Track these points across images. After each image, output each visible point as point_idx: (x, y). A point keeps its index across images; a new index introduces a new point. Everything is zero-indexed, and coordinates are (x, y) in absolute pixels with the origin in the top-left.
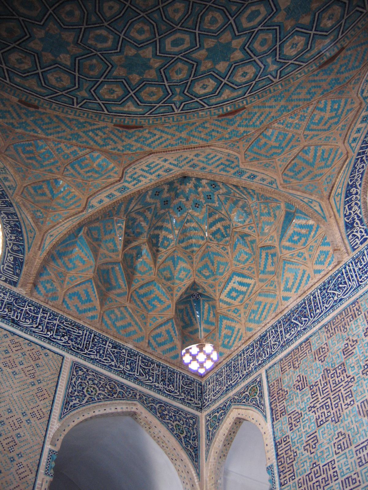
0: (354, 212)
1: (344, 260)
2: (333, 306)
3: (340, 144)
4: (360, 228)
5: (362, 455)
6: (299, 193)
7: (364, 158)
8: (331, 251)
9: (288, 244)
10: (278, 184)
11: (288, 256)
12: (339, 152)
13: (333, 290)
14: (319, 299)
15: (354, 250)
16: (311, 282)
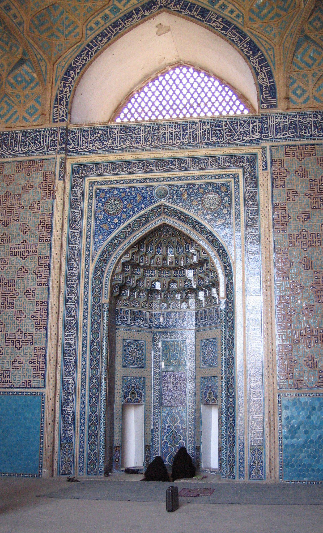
0: (66, 92)
1: (46, 125)
2: (26, 153)
3: (80, 23)
4: (64, 109)
5: (13, 250)
6: (36, 46)
7: (90, 53)
8: (39, 111)
9: (12, 81)
10: (25, 28)
11: (9, 92)
12: (77, 30)
13: (30, 141)
14: (19, 140)
15: (54, 122)
16: (18, 124)
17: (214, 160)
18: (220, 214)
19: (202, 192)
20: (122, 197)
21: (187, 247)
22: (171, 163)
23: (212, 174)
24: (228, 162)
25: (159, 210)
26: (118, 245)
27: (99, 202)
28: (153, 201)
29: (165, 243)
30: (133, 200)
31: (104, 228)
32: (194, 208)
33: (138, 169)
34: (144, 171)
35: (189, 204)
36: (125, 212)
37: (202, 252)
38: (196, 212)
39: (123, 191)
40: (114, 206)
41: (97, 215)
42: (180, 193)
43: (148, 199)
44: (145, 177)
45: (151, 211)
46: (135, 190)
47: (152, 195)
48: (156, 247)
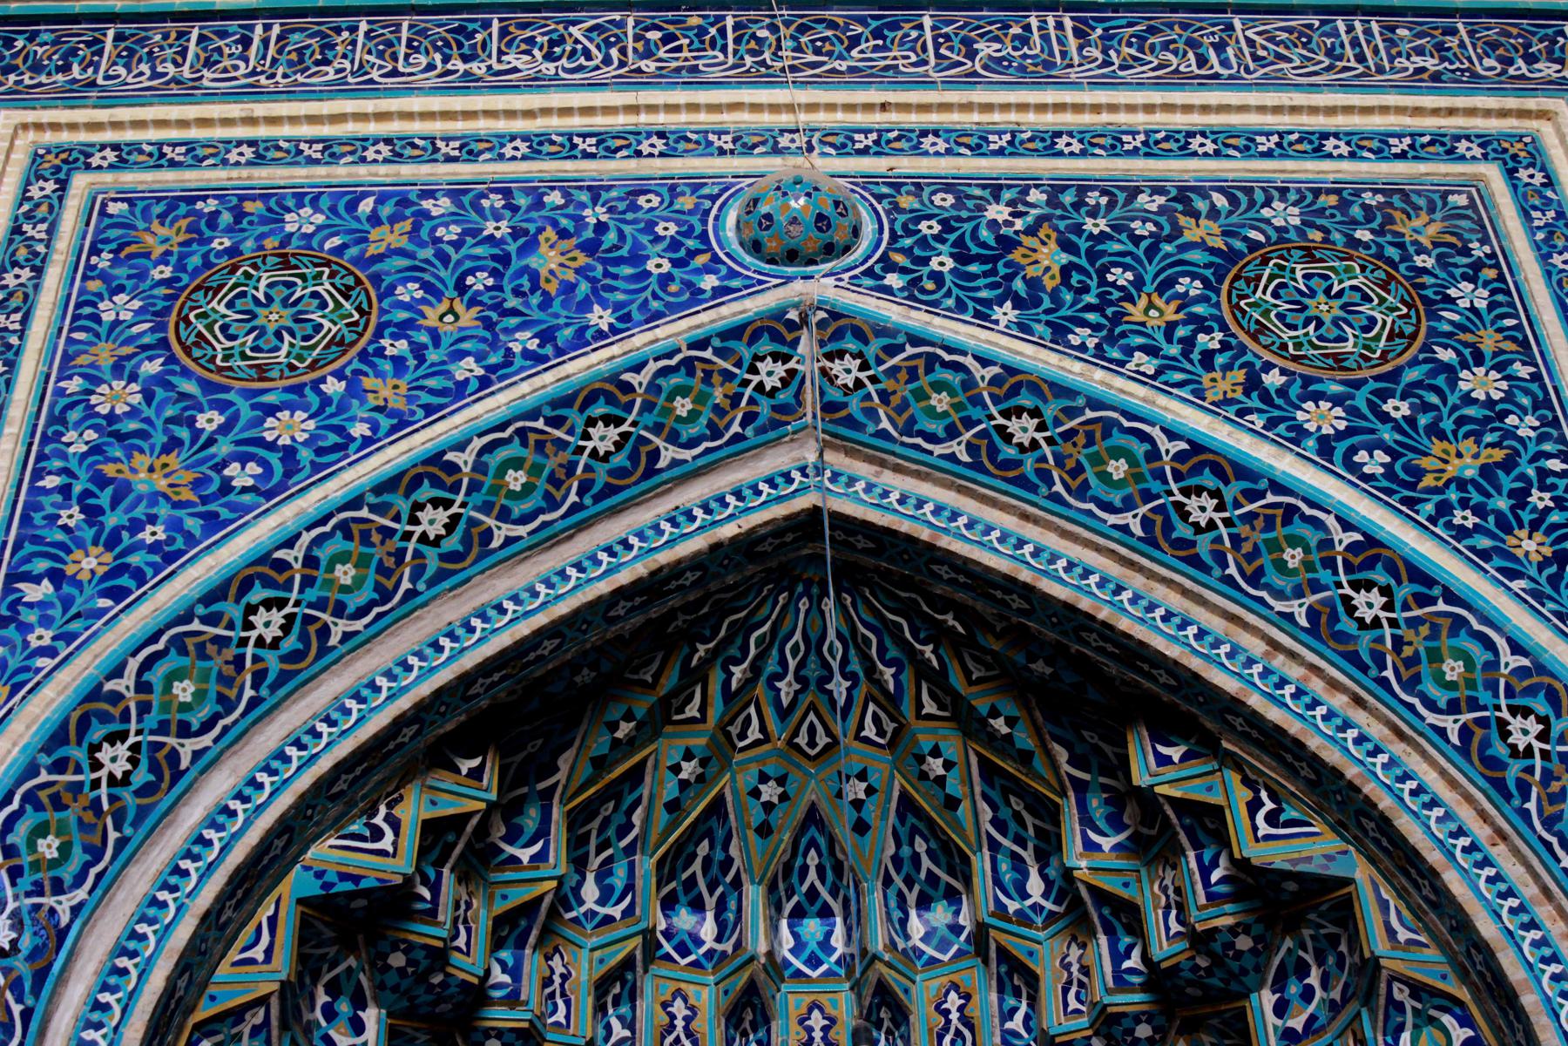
17: (1285, 35)
18: (1434, 399)
19: (1218, 243)
20: (373, 250)
21: (1008, 877)
22: (877, 34)
23: (1285, 121)
24: (1420, 51)
25: (771, 373)
26: (284, 677)
27: (121, 289)
28: (709, 282)
29: (764, 830)
30: (494, 273)
31: (143, 482)
32: (1152, 351)
33: (549, 57)
34: (611, 71)
35: (1092, 317)
36: (399, 362)
37: (1254, 806)
38: (1178, 377)
39: (386, 210)
40: (274, 317)
41: (74, 385)
42: (985, 234)
43: (657, 264)
44: (621, 121)
45: (684, 366)
46: (515, 209)
47: (691, 243)
48: (667, 869)
